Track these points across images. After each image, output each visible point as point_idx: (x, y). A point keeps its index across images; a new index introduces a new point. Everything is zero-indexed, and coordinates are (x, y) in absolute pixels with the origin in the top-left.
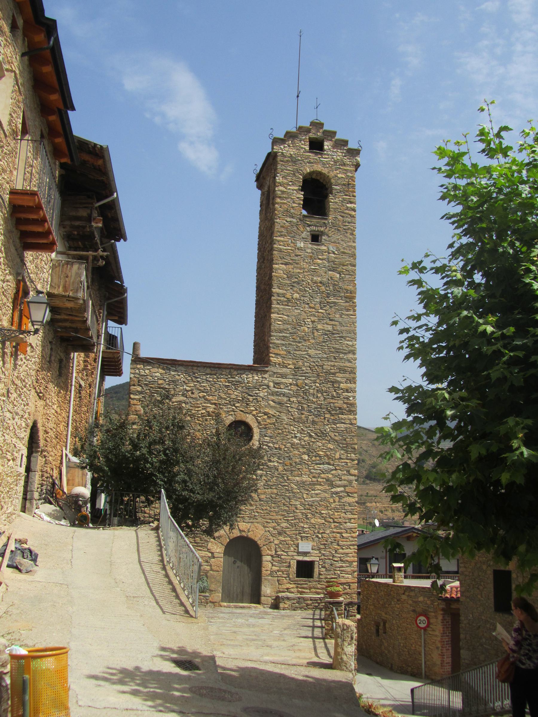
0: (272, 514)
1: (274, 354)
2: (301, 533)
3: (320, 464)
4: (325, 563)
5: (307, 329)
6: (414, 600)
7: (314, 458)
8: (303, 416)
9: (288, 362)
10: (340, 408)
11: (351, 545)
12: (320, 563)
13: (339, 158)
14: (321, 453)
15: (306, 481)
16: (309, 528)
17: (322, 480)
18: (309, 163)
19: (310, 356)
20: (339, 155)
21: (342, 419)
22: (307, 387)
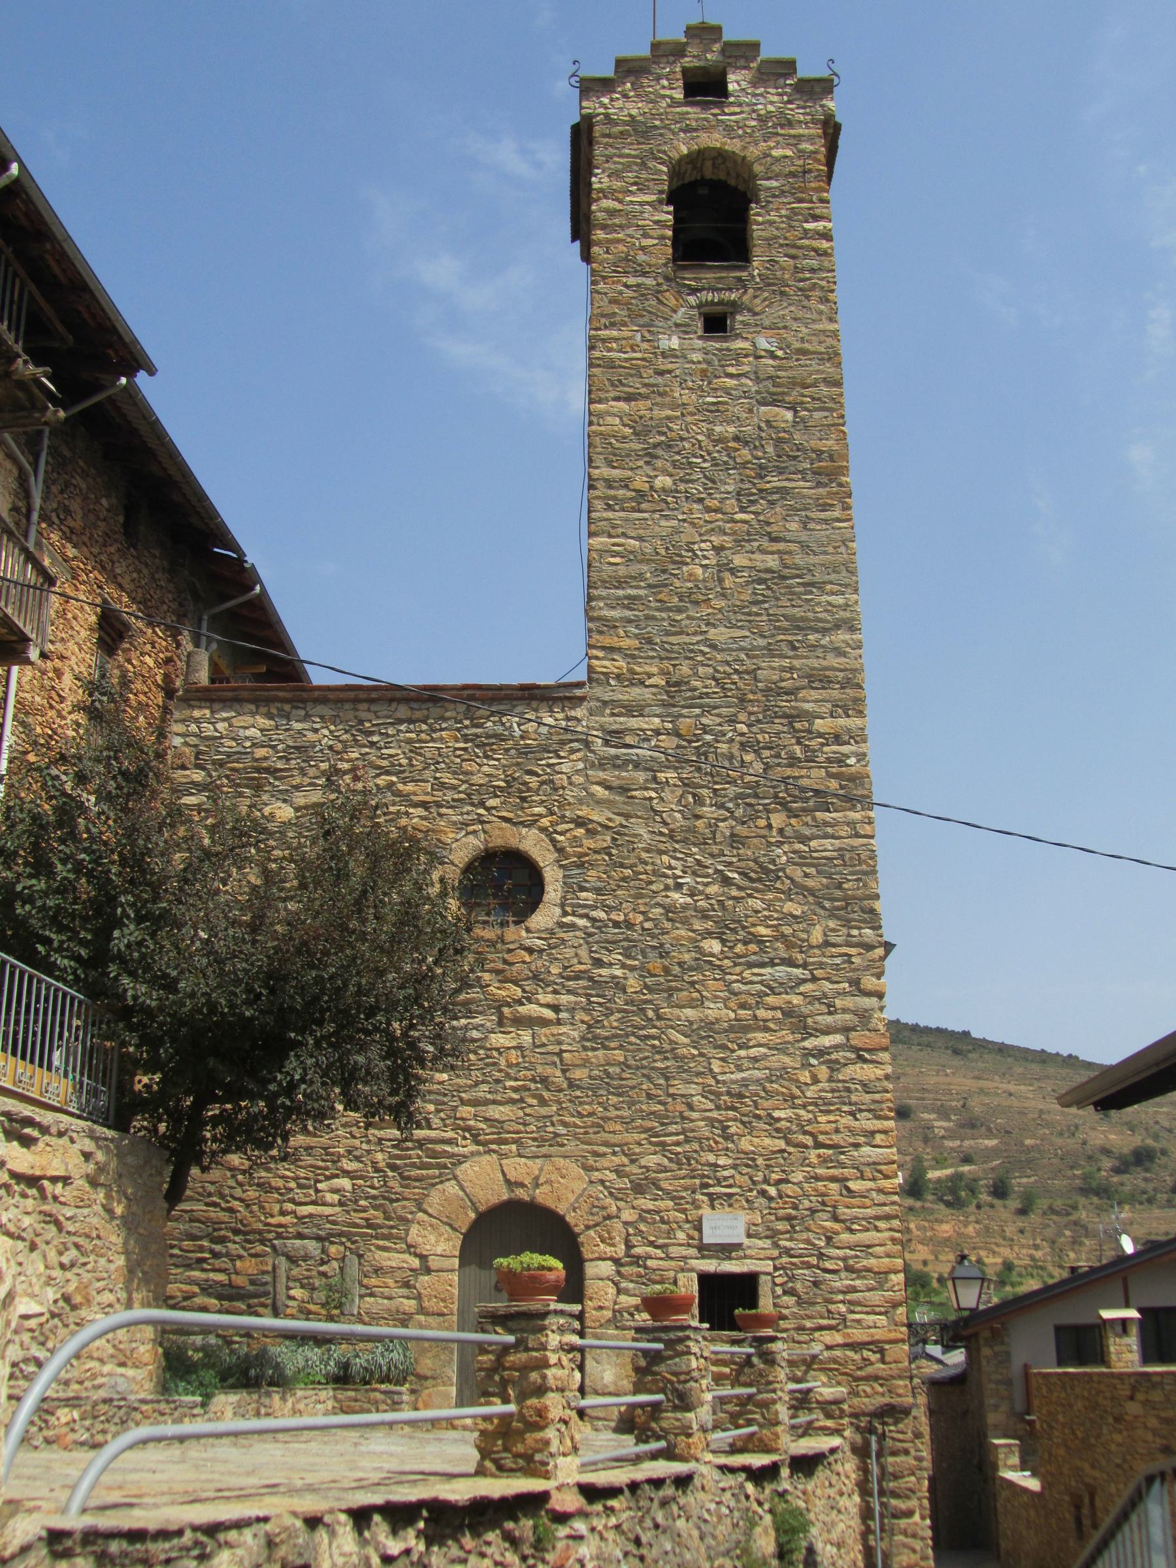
0: (611, 1126)
1: (603, 648)
2: (707, 1186)
3: (762, 965)
4: (792, 1278)
5: (699, 571)
6: (1163, 1414)
7: (739, 949)
8: (700, 823)
9: (647, 669)
10: (817, 792)
11: (878, 1218)
12: (778, 1280)
13: (771, 108)
14: (762, 930)
15: (718, 1020)
16: (735, 1167)
17: (769, 1014)
18: (684, 131)
19: (713, 647)
20: (771, 100)
21: (826, 824)
22: (708, 737)
